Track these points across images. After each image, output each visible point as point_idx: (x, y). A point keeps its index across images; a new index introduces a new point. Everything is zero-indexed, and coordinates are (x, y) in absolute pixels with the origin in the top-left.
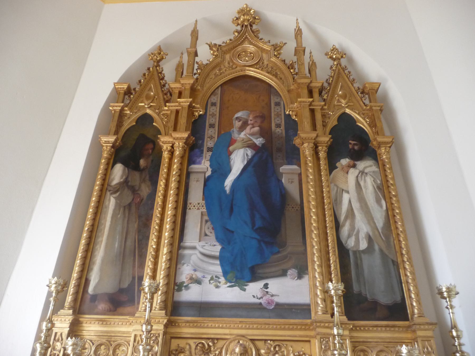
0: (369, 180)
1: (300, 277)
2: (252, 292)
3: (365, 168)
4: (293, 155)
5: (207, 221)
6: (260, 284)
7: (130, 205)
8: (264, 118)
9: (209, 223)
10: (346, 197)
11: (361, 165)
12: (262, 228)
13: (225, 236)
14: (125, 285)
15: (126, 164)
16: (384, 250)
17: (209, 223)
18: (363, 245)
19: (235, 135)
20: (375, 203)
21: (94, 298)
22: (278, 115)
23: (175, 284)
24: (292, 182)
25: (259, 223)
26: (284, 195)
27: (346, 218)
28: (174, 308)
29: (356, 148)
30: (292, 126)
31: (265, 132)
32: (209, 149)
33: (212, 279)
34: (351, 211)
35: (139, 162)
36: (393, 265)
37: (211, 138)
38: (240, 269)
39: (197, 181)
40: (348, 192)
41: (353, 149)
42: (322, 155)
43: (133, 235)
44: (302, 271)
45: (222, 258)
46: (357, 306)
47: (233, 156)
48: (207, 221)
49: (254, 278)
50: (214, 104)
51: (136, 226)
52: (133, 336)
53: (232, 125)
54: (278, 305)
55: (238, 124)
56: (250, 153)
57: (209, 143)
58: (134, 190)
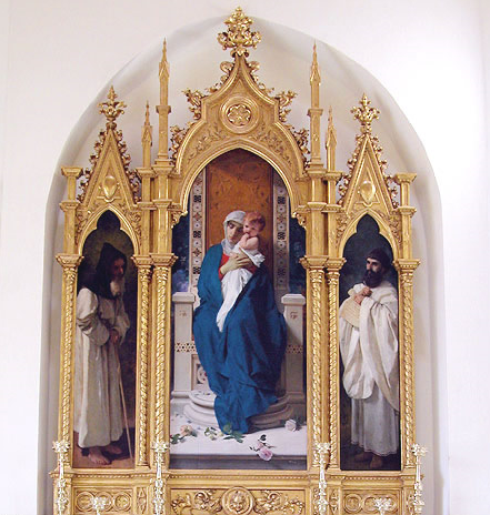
0: (384, 313)
1: (298, 428)
2: (249, 444)
3: (382, 297)
4: (298, 280)
5: (198, 366)
6: (258, 435)
7: (107, 344)
8: (263, 223)
9: (201, 368)
10: (355, 334)
11: (378, 292)
12: (258, 367)
13: (219, 383)
14: (116, 438)
15: (94, 290)
16: (388, 398)
17: (201, 368)
18: (367, 393)
19: (227, 250)
20: (388, 345)
21: (86, 451)
22: (281, 219)
23: (170, 437)
24: (295, 317)
25: (256, 369)
26: (284, 331)
27: (353, 361)
28: (174, 461)
29: (375, 268)
30: (298, 235)
31: (265, 246)
32: (196, 271)
33: (208, 430)
34: (358, 355)
35: (109, 286)
36: (395, 415)
37: (197, 252)
38: (236, 420)
39: (184, 314)
40: (358, 329)
41: (371, 270)
42: (334, 282)
43: (117, 383)
44: (301, 421)
45: (216, 408)
46: (353, 456)
47: (224, 281)
48: (198, 366)
49: (251, 431)
50: (197, 199)
51: (118, 370)
52: (135, 488)
53: (222, 234)
54: (274, 456)
55: (230, 232)
56: (246, 275)
57: (195, 261)
58: (109, 325)
